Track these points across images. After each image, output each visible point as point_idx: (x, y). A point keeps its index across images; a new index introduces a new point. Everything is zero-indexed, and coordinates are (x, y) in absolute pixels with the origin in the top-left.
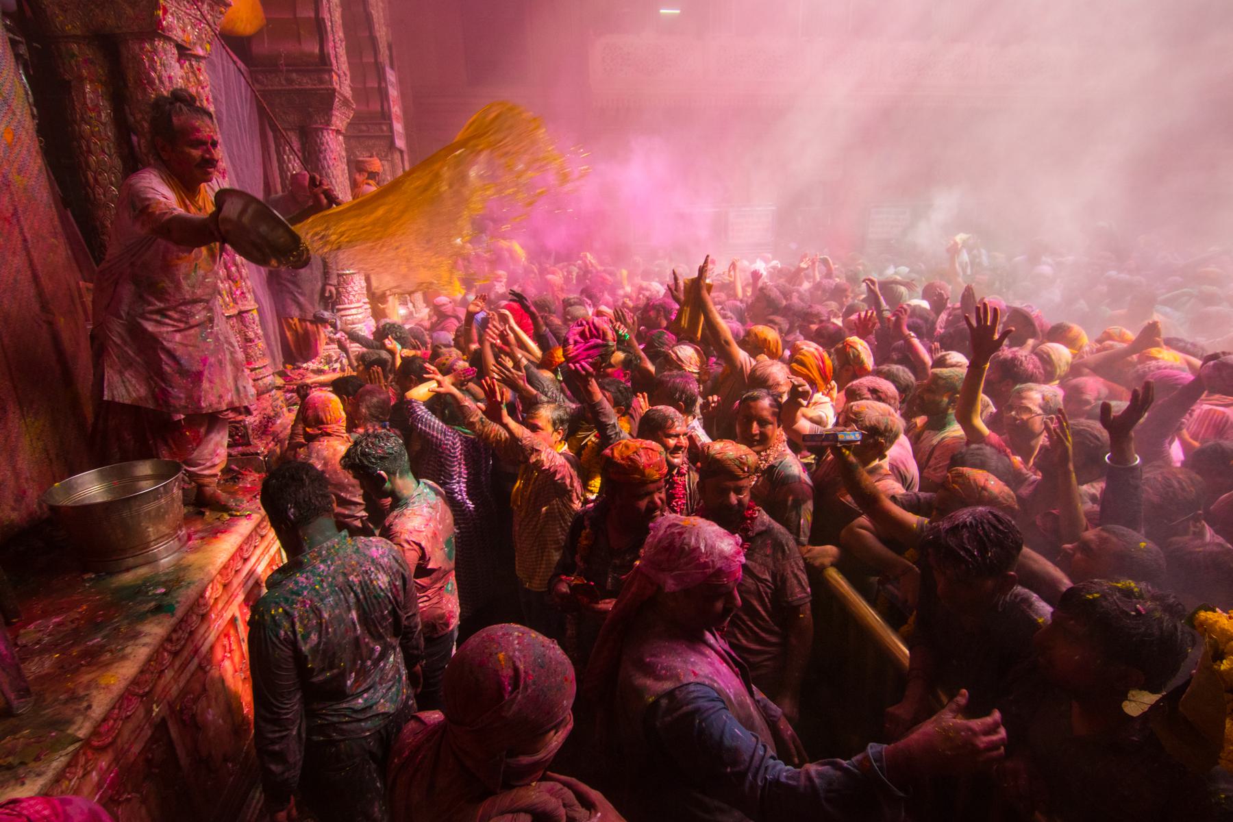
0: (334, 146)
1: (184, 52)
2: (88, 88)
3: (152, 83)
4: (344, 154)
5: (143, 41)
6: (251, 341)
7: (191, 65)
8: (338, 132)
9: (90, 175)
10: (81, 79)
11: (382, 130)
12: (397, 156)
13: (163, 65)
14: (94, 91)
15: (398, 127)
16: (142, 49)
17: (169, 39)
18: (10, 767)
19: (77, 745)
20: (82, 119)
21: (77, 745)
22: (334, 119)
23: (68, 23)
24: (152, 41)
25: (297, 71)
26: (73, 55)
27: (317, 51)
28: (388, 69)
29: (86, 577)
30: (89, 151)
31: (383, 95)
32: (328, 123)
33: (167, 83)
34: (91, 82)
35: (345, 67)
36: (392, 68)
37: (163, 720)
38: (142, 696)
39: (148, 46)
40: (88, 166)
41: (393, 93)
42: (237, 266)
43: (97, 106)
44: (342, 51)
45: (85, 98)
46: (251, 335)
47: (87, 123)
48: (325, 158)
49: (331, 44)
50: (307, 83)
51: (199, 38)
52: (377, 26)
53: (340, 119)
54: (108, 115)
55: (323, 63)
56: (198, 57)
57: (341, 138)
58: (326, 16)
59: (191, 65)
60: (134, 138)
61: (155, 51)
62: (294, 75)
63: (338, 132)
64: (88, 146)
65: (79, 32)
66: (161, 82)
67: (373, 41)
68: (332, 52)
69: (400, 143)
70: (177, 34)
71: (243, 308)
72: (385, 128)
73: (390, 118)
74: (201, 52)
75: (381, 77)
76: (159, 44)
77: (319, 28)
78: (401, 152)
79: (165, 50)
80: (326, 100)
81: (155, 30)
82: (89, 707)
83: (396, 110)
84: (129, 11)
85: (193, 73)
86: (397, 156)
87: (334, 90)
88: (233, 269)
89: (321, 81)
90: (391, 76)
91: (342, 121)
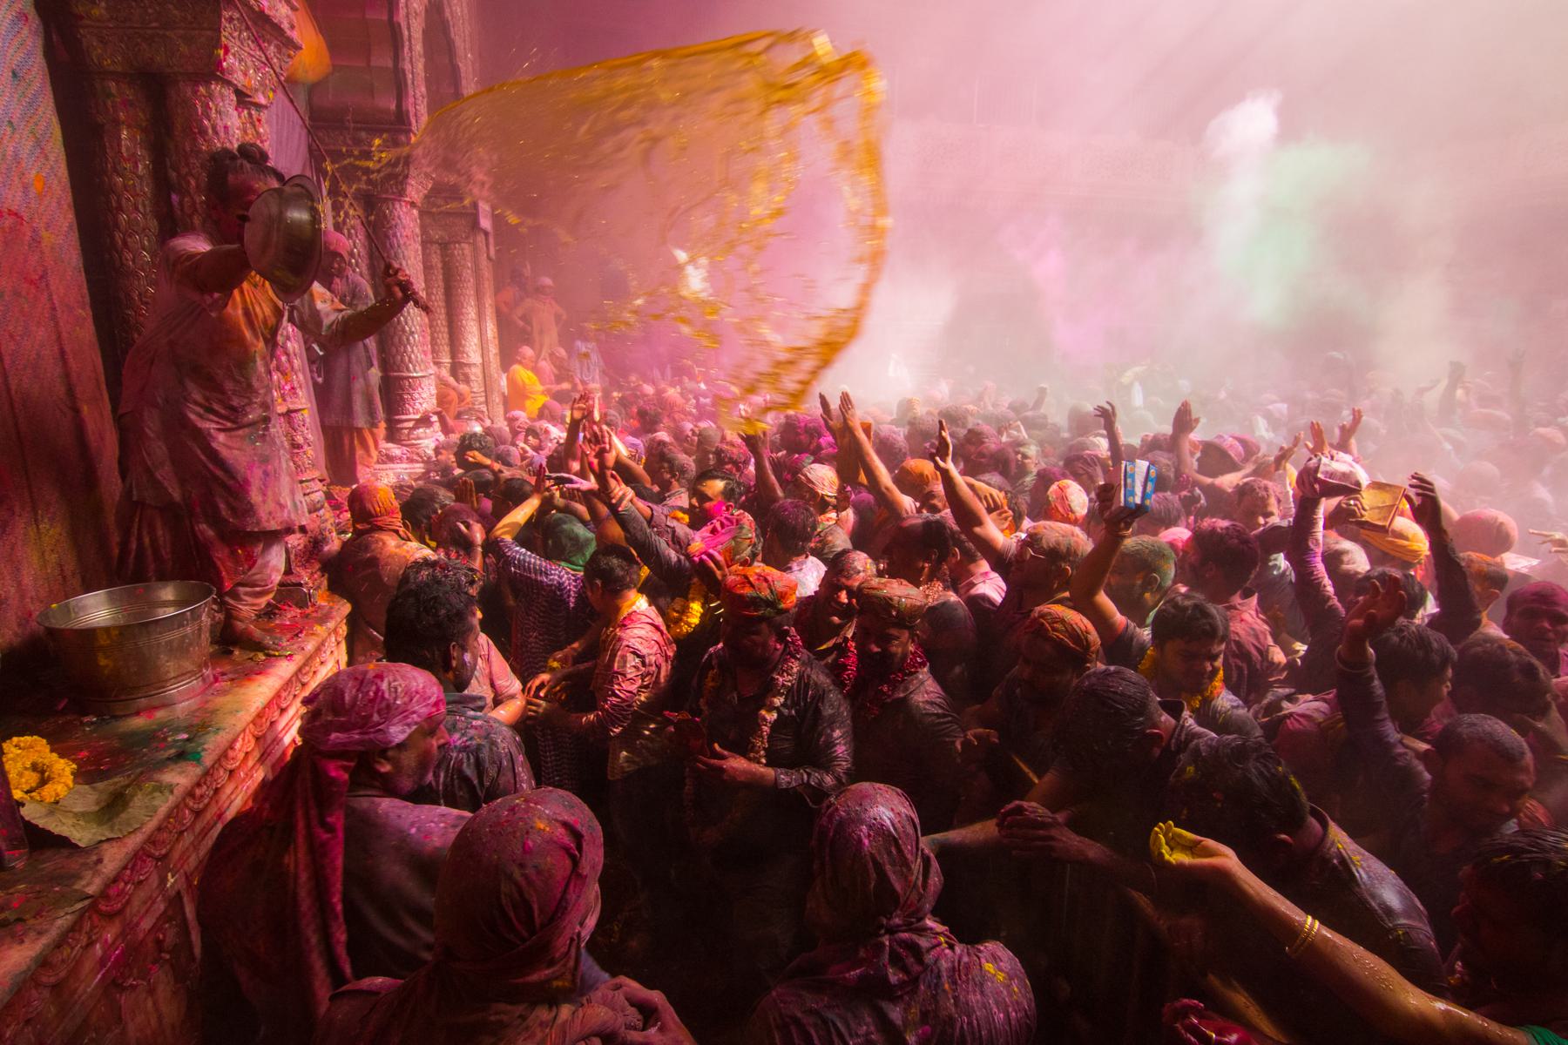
1: (243, 99)
2: (124, 134)
3: (203, 132)
4: (418, 230)
5: (197, 83)
6: (299, 447)
7: (250, 115)
8: (413, 204)
9: (118, 236)
10: (117, 123)
12: (481, 238)
13: (219, 112)
14: (132, 138)
17: (228, 83)
18: (4, 924)
19: (87, 902)
20: (115, 170)
21: (87, 902)
22: (409, 189)
23: (105, 55)
24: (207, 83)
26: (109, 95)
27: (393, 107)
29: (86, 719)
30: (120, 209)
32: (402, 193)
33: (222, 134)
34: (129, 127)
37: (179, 893)
38: (158, 859)
39: (202, 89)
40: (117, 225)
42: (288, 355)
43: (134, 155)
44: (423, 108)
45: (119, 145)
46: (300, 439)
47: (119, 175)
48: (395, 235)
49: (411, 100)
51: (262, 83)
52: (464, 82)
54: (146, 167)
56: (259, 106)
57: (415, 212)
58: (407, 66)
59: (250, 115)
60: (175, 198)
61: (211, 96)
62: (363, 134)
63: (413, 204)
64: (119, 202)
65: (120, 69)
66: (216, 133)
68: (412, 110)
69: (486, 223)
70: (238, 78)
71: (292, 407)
74: (263, 101)
76: (216, 88)
78: (486, 234)
79: (222, 96)
81: (213, 72)
82: (100, 861)
84: (184, 49)
85: (252, 124)
86: (481, 238)
88: (284, 358)
91: (418, 192)
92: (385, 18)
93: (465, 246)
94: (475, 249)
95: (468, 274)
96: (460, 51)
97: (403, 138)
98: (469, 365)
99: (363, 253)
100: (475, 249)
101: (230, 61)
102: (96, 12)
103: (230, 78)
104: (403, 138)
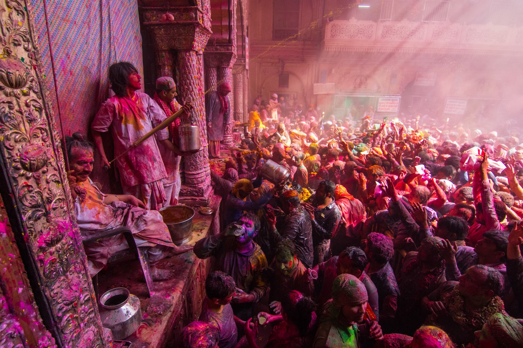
0: (229, 72)
3: (188, 67)
6: (205, 157)
8: (231, 68)
10: (164, 65)
11: (241, 62)
13: (192, 60)
15: (247, 60)
16: (186, 55)
17: (195, 51)
23: (163, 45)
24: (189, 51)
25: (220, 46)
26: (163, 57)
27: (228, 38)
28: (246, 38)
31: (243, 48)
32: (228, 65)
34: (168, 66)
35: (236, 43)
36: (247, 36)
39: (188, 54)
41: (247, 47)
44: (235, 37)
46: (206, 155)
50: (223, 50)
51: (202, 48)
53: (233, 62)
55: (230, 41)
56: (200, 54)
61: (190, 55)
62: (218, 47)
66: (191, 67)
67: (242, 26)
69: (247, 67)
72: (243, 61)
73: (245, 58)
75: (244, 41)
76: (191, 53)
77: (229, 29)
78: (247, 70)
80: (229, 56)
81: (191, 48)
83: (247, 53)
84: (184, 42)
86: (245, 72)
87: (232, 53)
89: (228, 49)
90: (247, 40)
92: (227, 9)
93: (241, 75)
94: (243, 74)
95: (241, 84)
96: (244, 11)
97: (230, 48)
98: (240, 113)
99: (216, 84)
100: (243, 74)
101: (196, 44)
102: (161, 33)
103: (195, 49)
104: (230, 48)
